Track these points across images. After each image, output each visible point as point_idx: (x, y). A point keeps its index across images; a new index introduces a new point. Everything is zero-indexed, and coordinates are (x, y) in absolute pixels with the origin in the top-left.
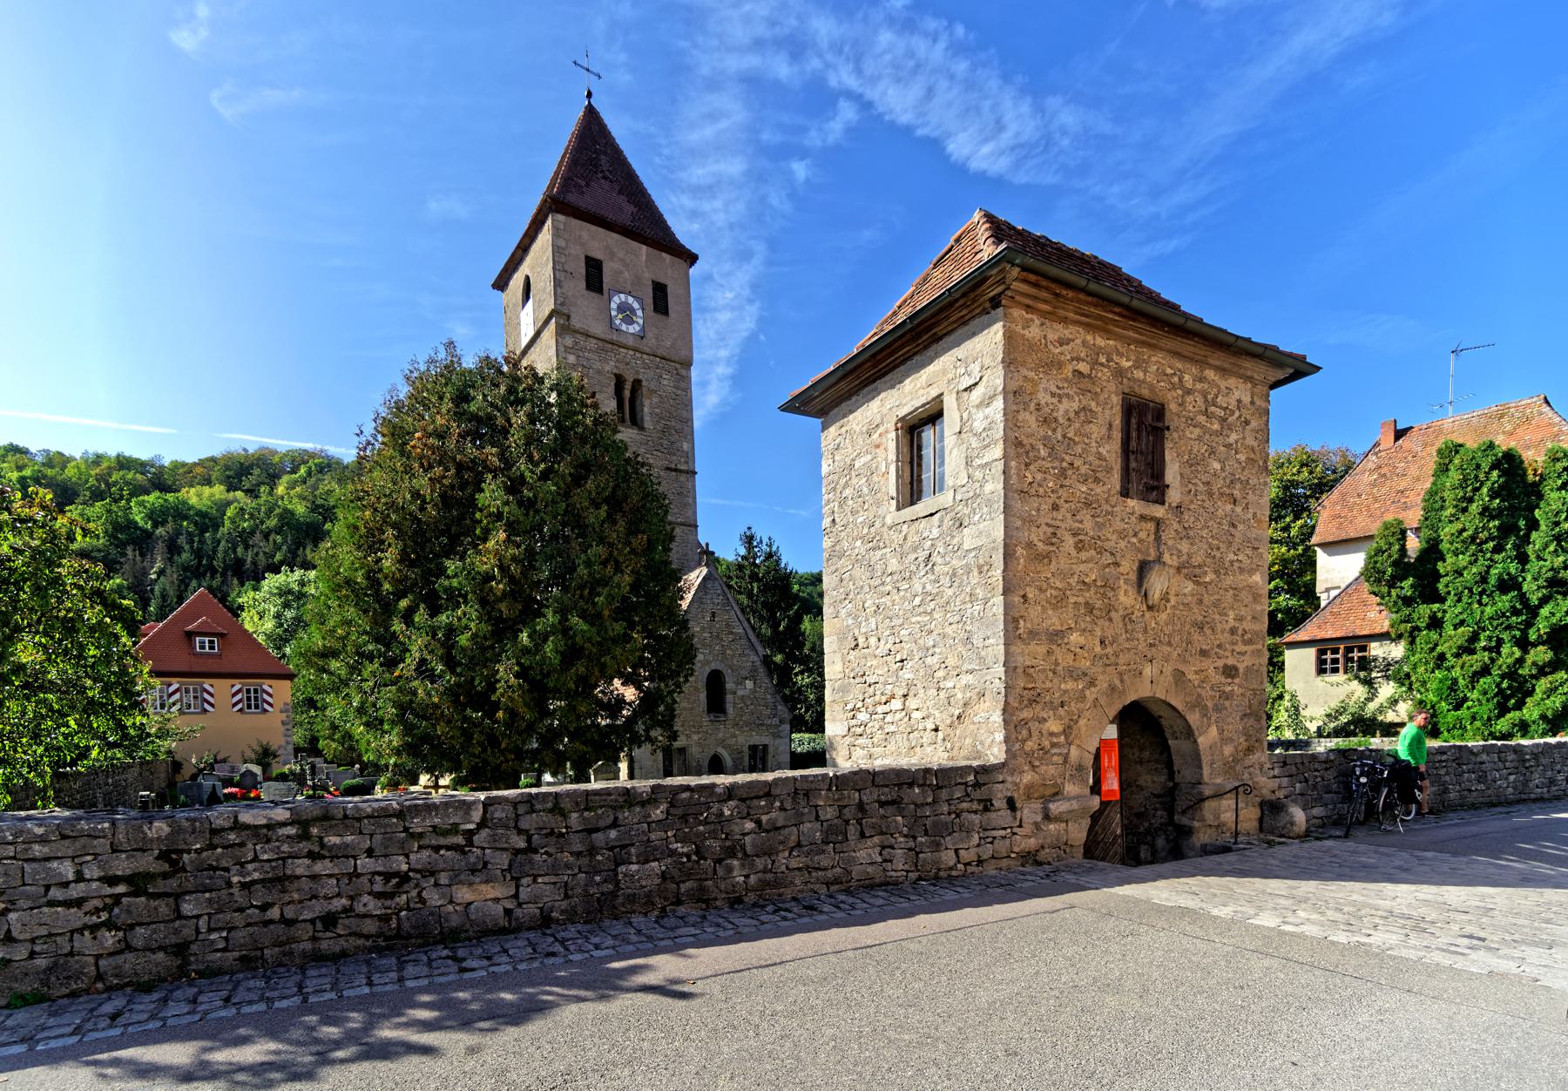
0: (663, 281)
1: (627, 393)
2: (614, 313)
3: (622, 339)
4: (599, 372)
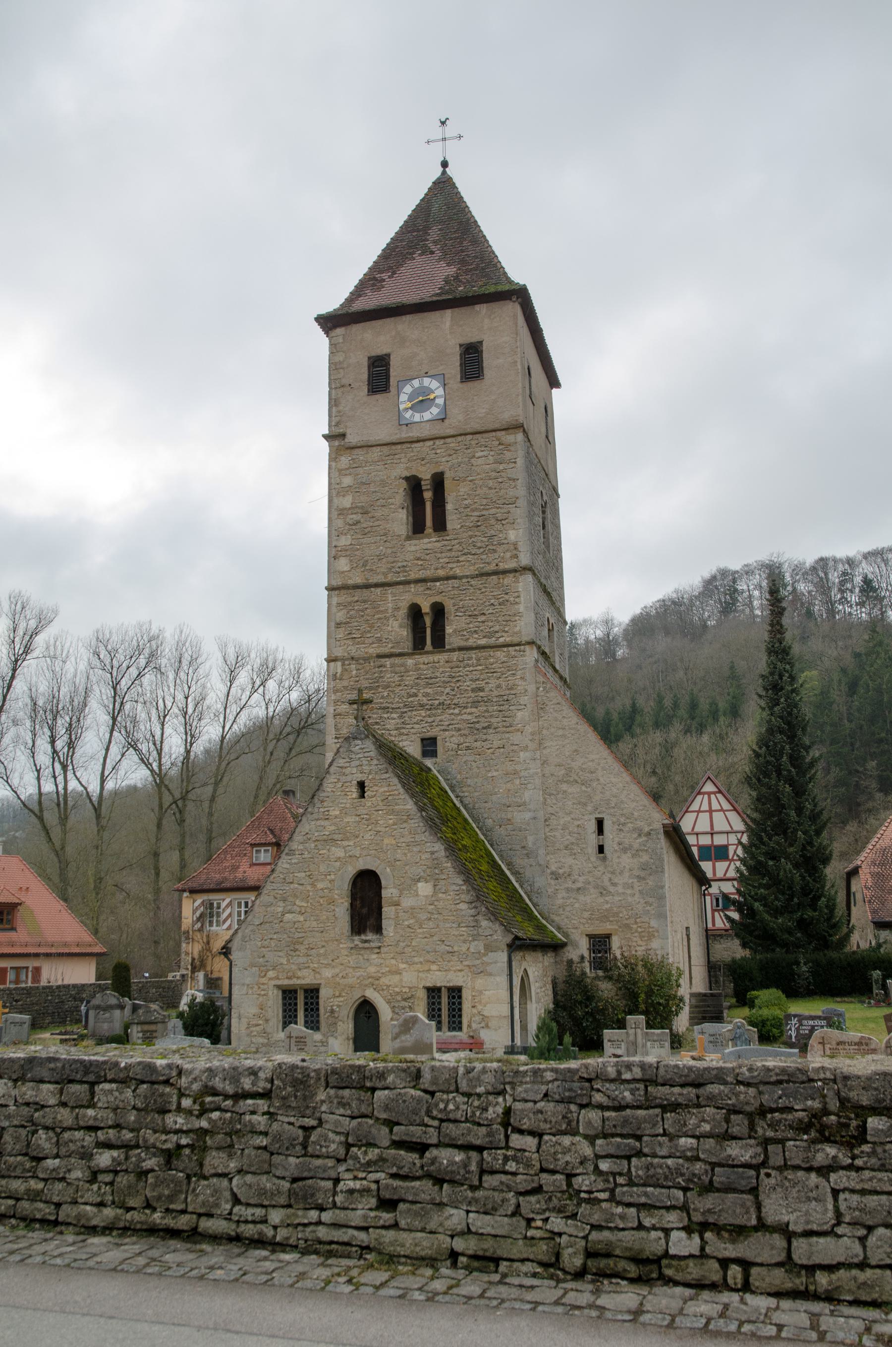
1: (428, 495)
2: (402, 407)
3: (415, 433)
4: (383, 483)
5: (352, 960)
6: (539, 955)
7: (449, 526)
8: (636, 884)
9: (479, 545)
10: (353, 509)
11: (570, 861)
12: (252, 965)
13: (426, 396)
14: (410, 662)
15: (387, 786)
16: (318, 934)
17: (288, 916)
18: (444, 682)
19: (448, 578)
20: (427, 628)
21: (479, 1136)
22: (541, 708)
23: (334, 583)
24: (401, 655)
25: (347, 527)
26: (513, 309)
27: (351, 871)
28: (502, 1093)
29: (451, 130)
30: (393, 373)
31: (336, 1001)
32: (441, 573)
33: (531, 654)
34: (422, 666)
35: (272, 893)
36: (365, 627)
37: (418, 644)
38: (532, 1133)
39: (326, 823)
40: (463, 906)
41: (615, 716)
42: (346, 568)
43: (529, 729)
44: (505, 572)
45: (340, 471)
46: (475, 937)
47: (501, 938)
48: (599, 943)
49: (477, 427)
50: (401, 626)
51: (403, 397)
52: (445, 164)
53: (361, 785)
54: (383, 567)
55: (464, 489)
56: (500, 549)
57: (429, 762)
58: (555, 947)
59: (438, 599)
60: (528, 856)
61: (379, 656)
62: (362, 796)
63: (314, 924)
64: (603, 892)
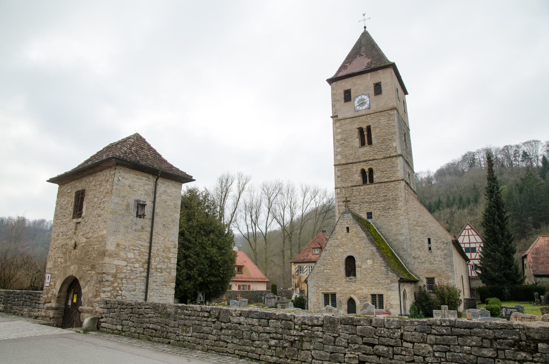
1: (365, 133)
3: (360, 114)
4: (351, 130)
5: (346, 285)
6: (409, 284)
7: (373, 143)
8: (443, 261)
10: (341, 139)
11: (419, 253)
12: (314, 286)
13: (363, 101)
14: (362, 188)
15: (356, 229)
19: (373, 160)
20: (367, 177)
21: (392, 342)
22: (407, 201)
23: (336, 164)
24: (359, 186)
26: (391, 71)
27: (345, 256)
28: (400, 328)
29: (366, 17)
30: (352, 95)
31: (341, 298)
32: (371, 158)
33: (403, 184)
36: (347, 177)
37: (365, 182)
38: (410, 342)
40: (383, 268)
41: (433, 204)
43: (403, 209)
44: (392, 157)
46: (387, 278)
47: (397, 279)
48: (430, 280)
49: (381, 110)
51: (356, 102)
52: (365, 28)
53: (348, 228)
55: (377, 130)
56: (391, 149)
57: (370, 221)
58: (415, 282)
59: (370, 167)
60: (404, 251)
61: (352, 186)
62: (348, 232)
64: (431, 263)
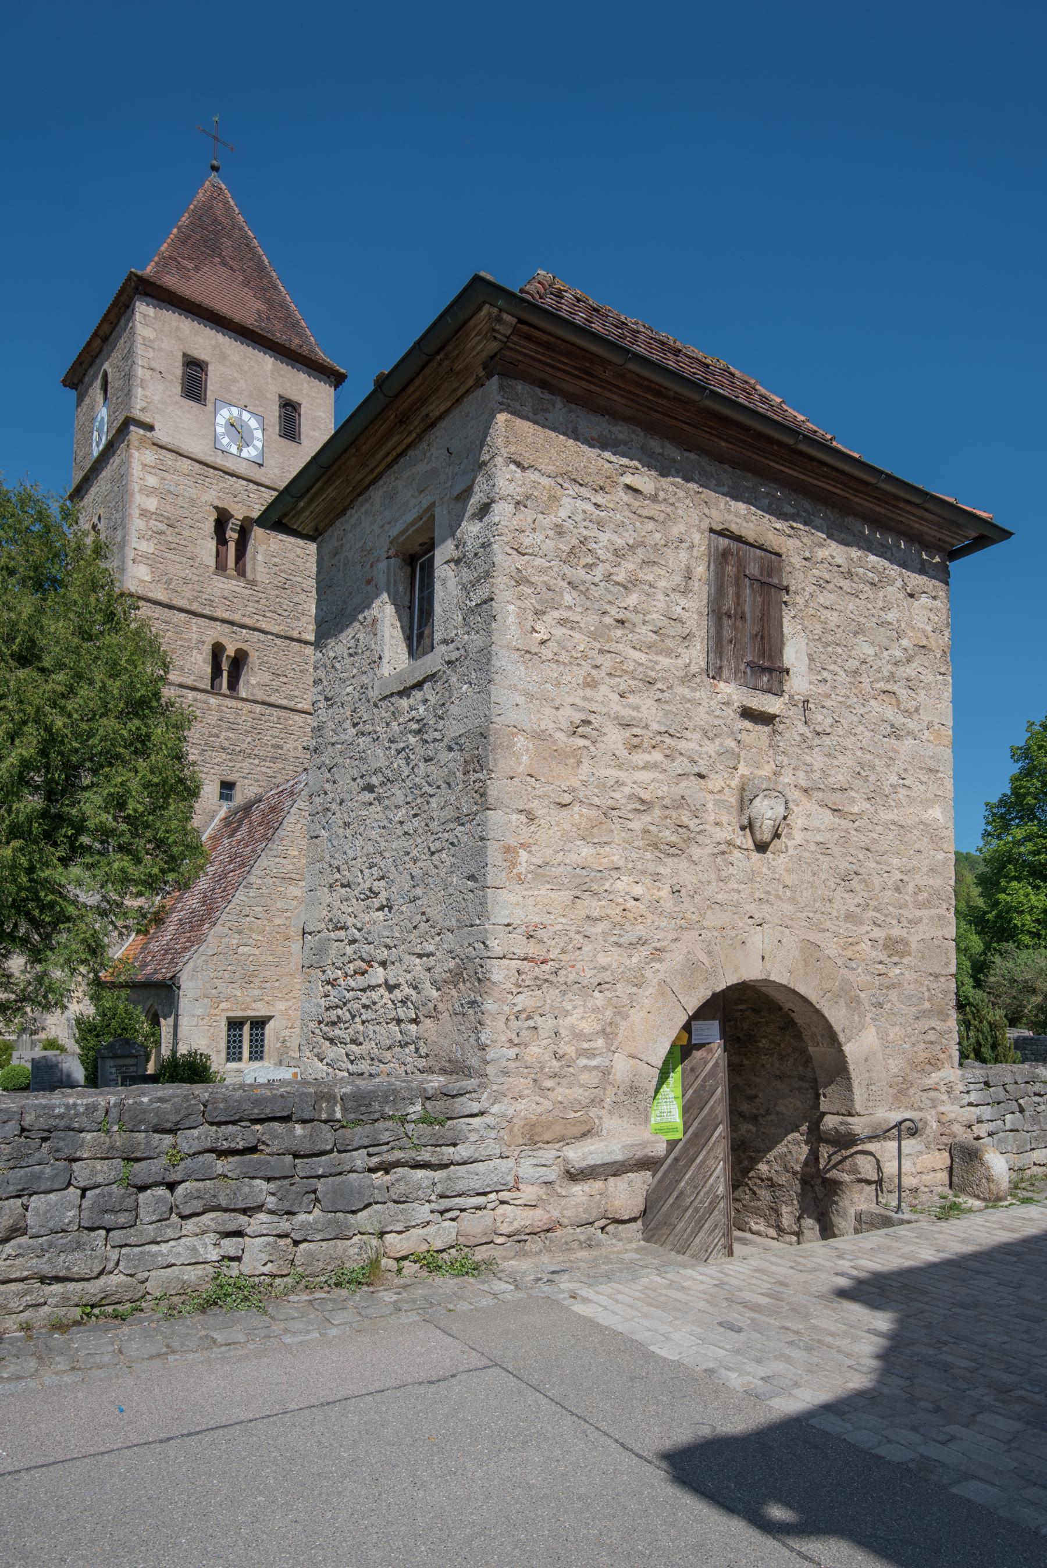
0: (294, 398)
3: (230, 465)
4: (193, 502)
9: (285, 607)
10: (157, 515)
14: (213, 701)
16: (273, 968)
17: (241, 949)
18: (246, 730)
19: (255, 629)
25: (150, 533)
34: (225, 709)
35: (228, 924)
39: (284, 861)
42: (148, 578)
45: (144, 465)
50: (204, 662)
54: (188, 592)
63: (270, 958)
